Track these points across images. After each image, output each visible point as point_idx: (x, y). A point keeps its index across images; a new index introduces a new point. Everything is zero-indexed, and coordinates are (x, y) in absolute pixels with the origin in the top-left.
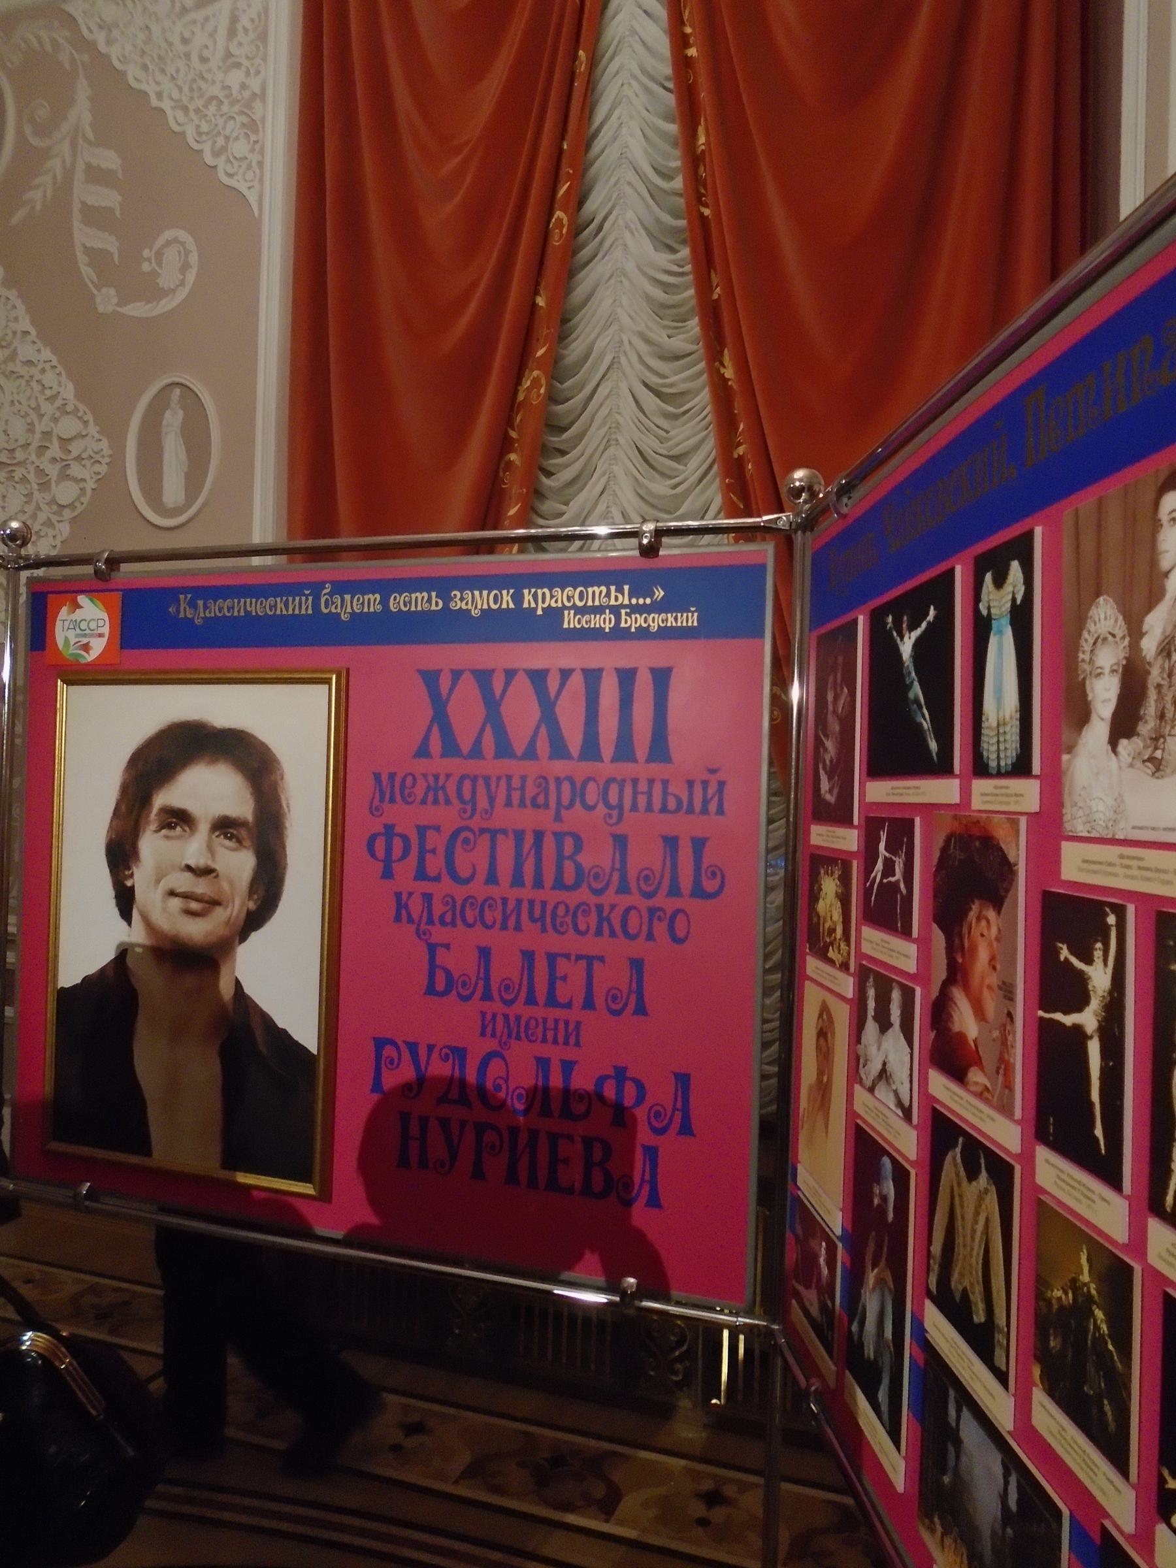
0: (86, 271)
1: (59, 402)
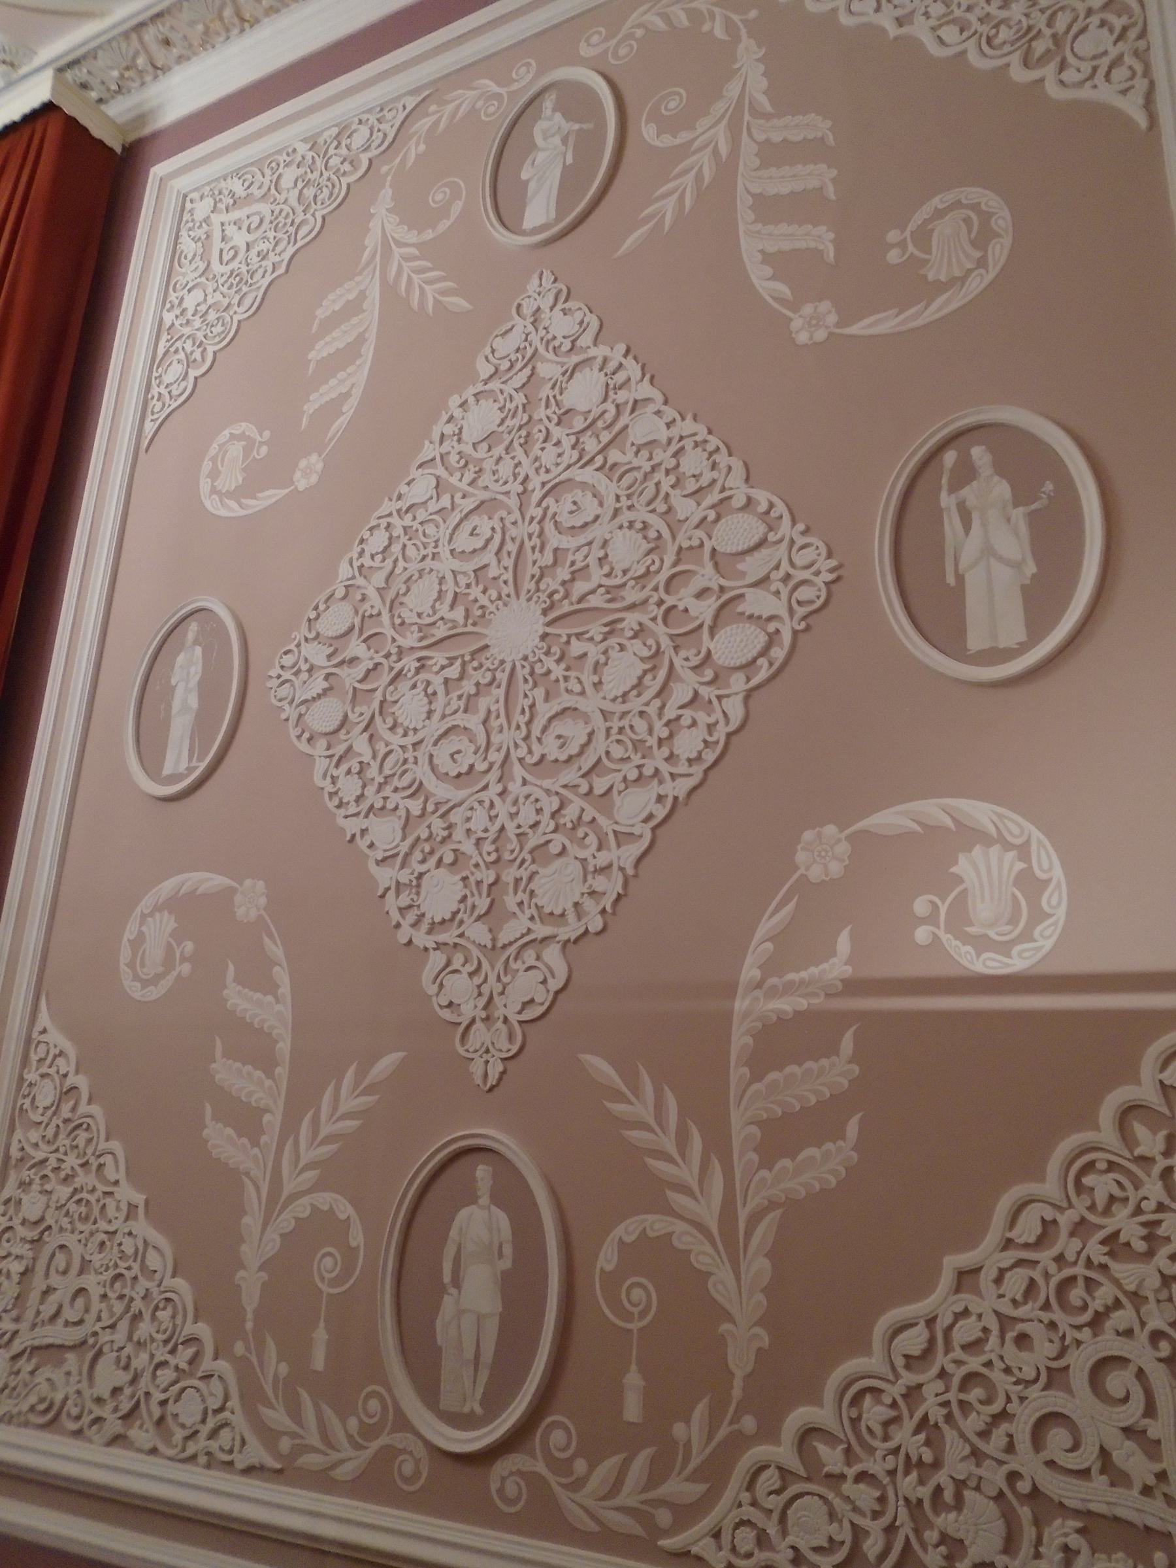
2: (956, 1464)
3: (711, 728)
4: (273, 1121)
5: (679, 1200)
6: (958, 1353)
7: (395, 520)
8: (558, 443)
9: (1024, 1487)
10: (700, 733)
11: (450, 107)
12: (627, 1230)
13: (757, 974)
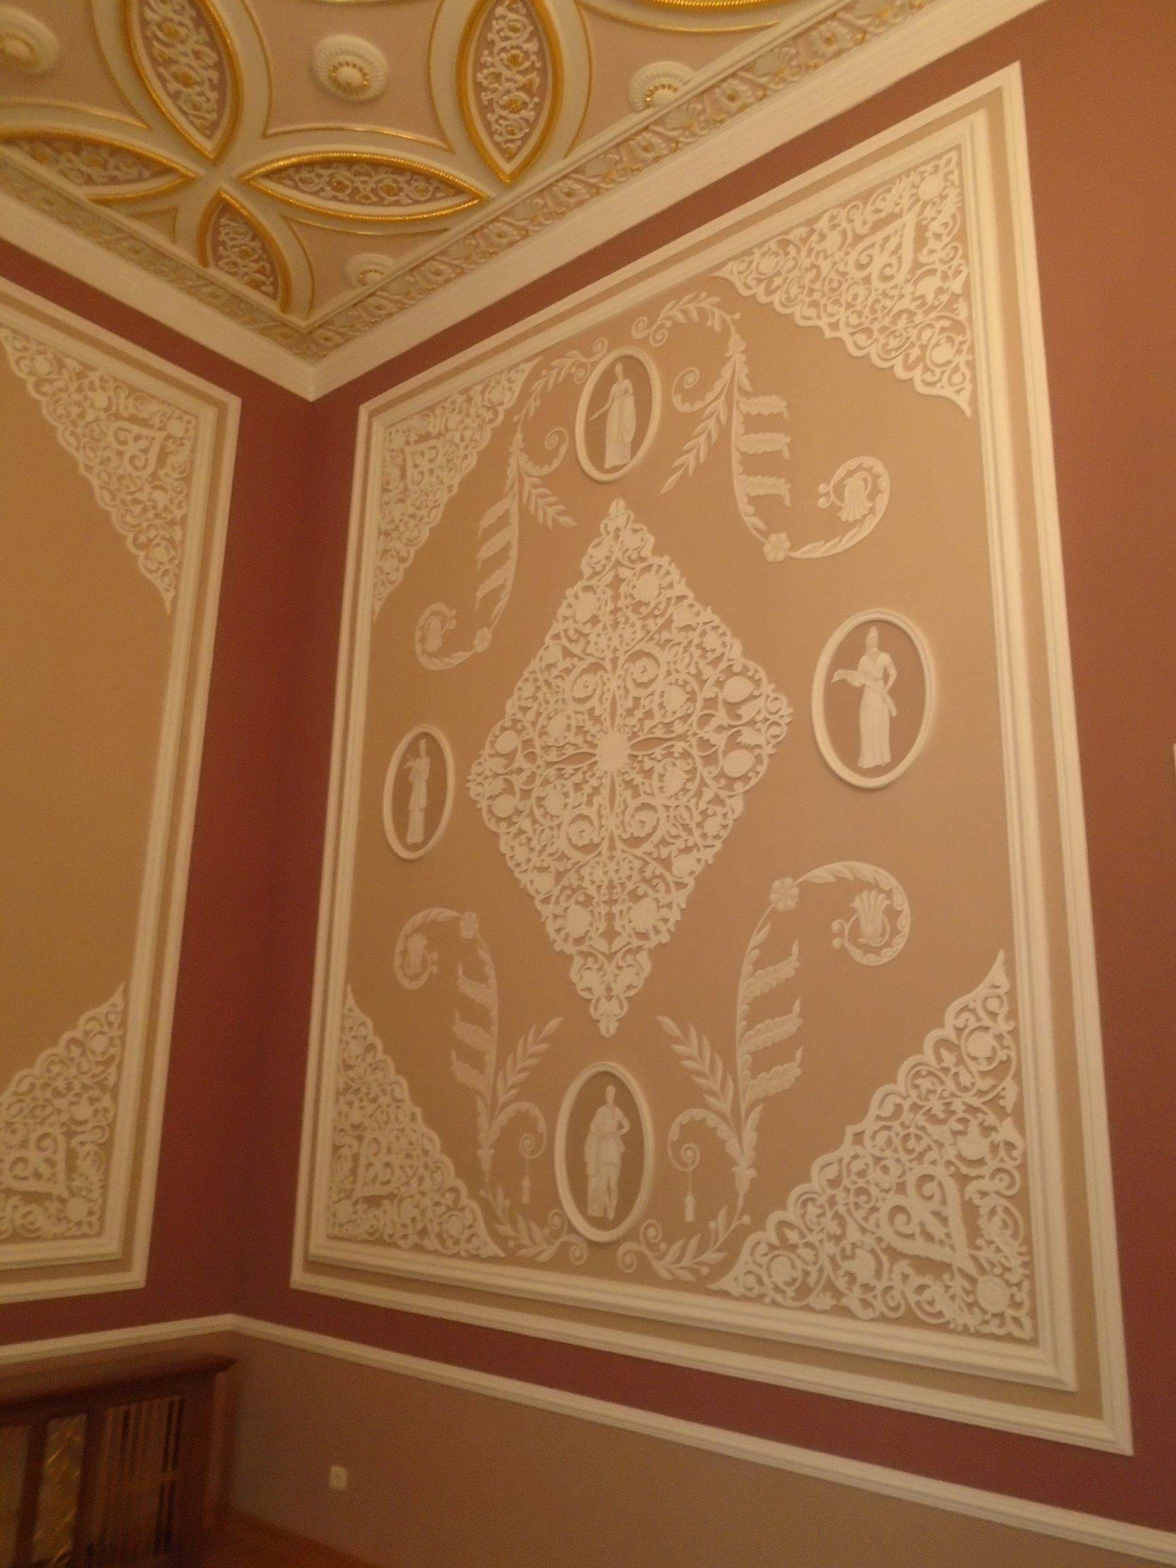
0: (753, 522)
1: (723, 665)
2: (853, 1235)
3: (725, 815)
4: (491, 1058)
5: (712, 1100)
6: (854, 1178)
7: (539, 675)
8: (633, 625)
9: (884, 1245)
10: (719, 820)
11: (555, 372)
12: (684, 1118)
13: (751, 967)
